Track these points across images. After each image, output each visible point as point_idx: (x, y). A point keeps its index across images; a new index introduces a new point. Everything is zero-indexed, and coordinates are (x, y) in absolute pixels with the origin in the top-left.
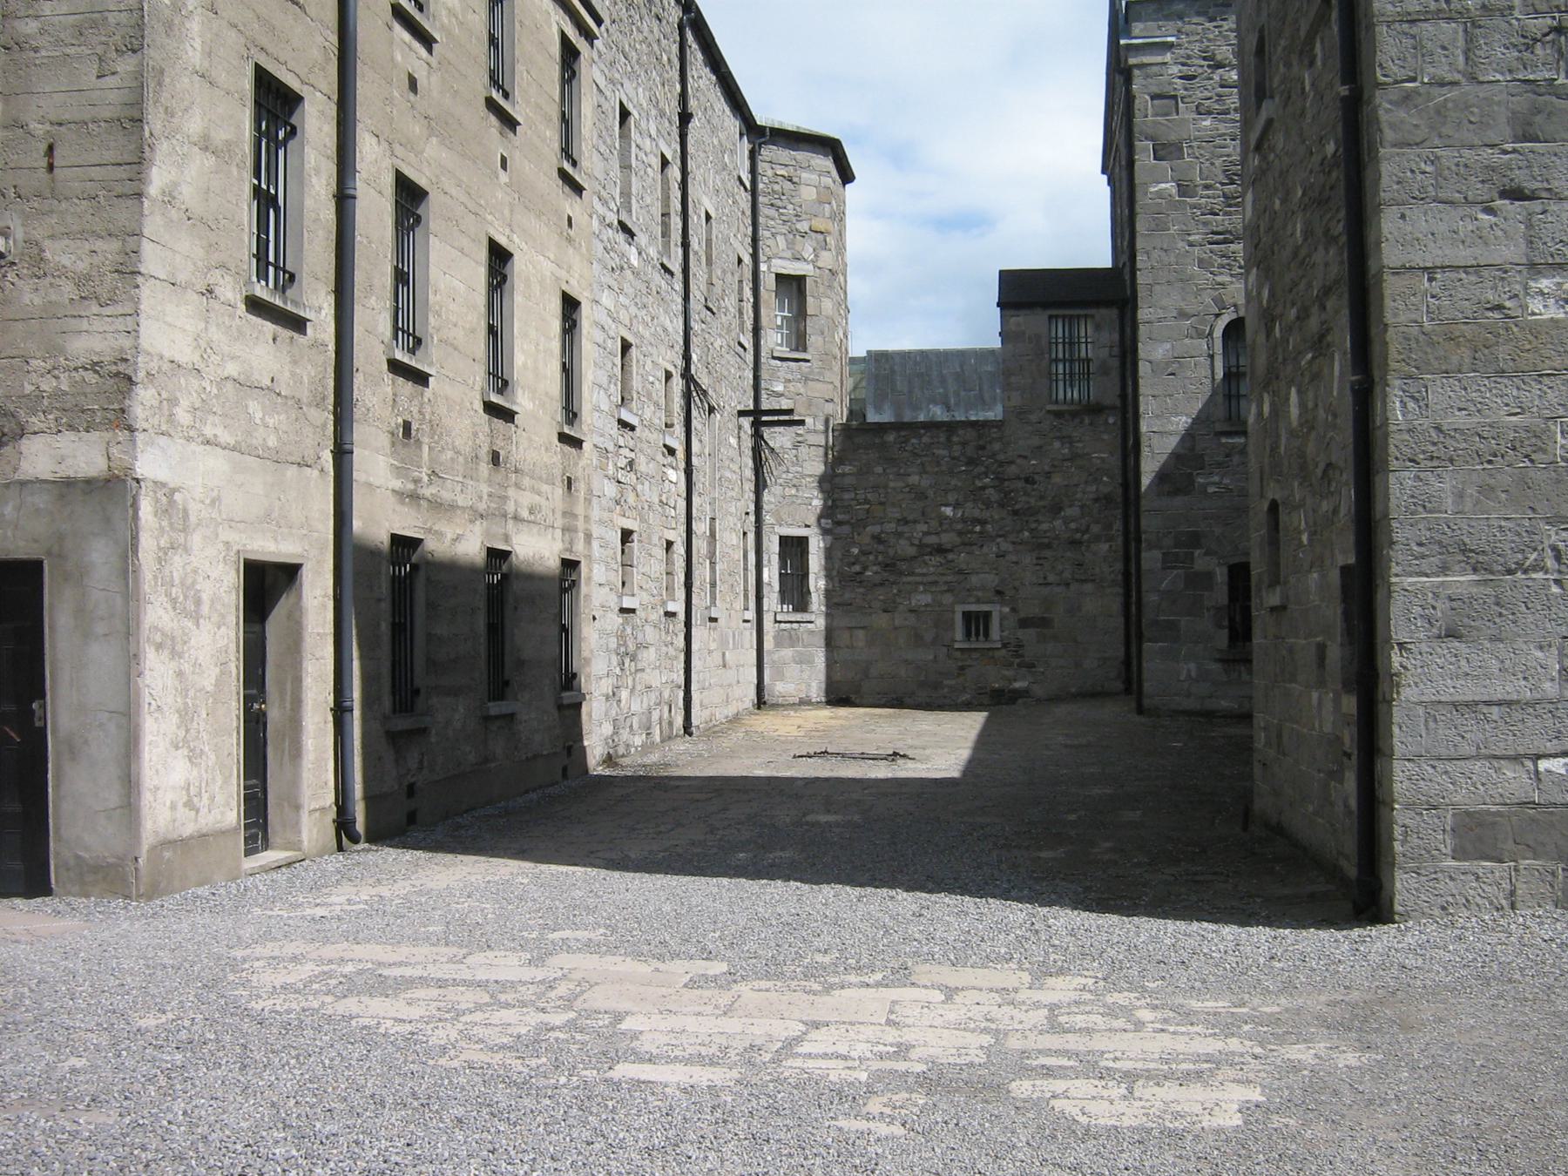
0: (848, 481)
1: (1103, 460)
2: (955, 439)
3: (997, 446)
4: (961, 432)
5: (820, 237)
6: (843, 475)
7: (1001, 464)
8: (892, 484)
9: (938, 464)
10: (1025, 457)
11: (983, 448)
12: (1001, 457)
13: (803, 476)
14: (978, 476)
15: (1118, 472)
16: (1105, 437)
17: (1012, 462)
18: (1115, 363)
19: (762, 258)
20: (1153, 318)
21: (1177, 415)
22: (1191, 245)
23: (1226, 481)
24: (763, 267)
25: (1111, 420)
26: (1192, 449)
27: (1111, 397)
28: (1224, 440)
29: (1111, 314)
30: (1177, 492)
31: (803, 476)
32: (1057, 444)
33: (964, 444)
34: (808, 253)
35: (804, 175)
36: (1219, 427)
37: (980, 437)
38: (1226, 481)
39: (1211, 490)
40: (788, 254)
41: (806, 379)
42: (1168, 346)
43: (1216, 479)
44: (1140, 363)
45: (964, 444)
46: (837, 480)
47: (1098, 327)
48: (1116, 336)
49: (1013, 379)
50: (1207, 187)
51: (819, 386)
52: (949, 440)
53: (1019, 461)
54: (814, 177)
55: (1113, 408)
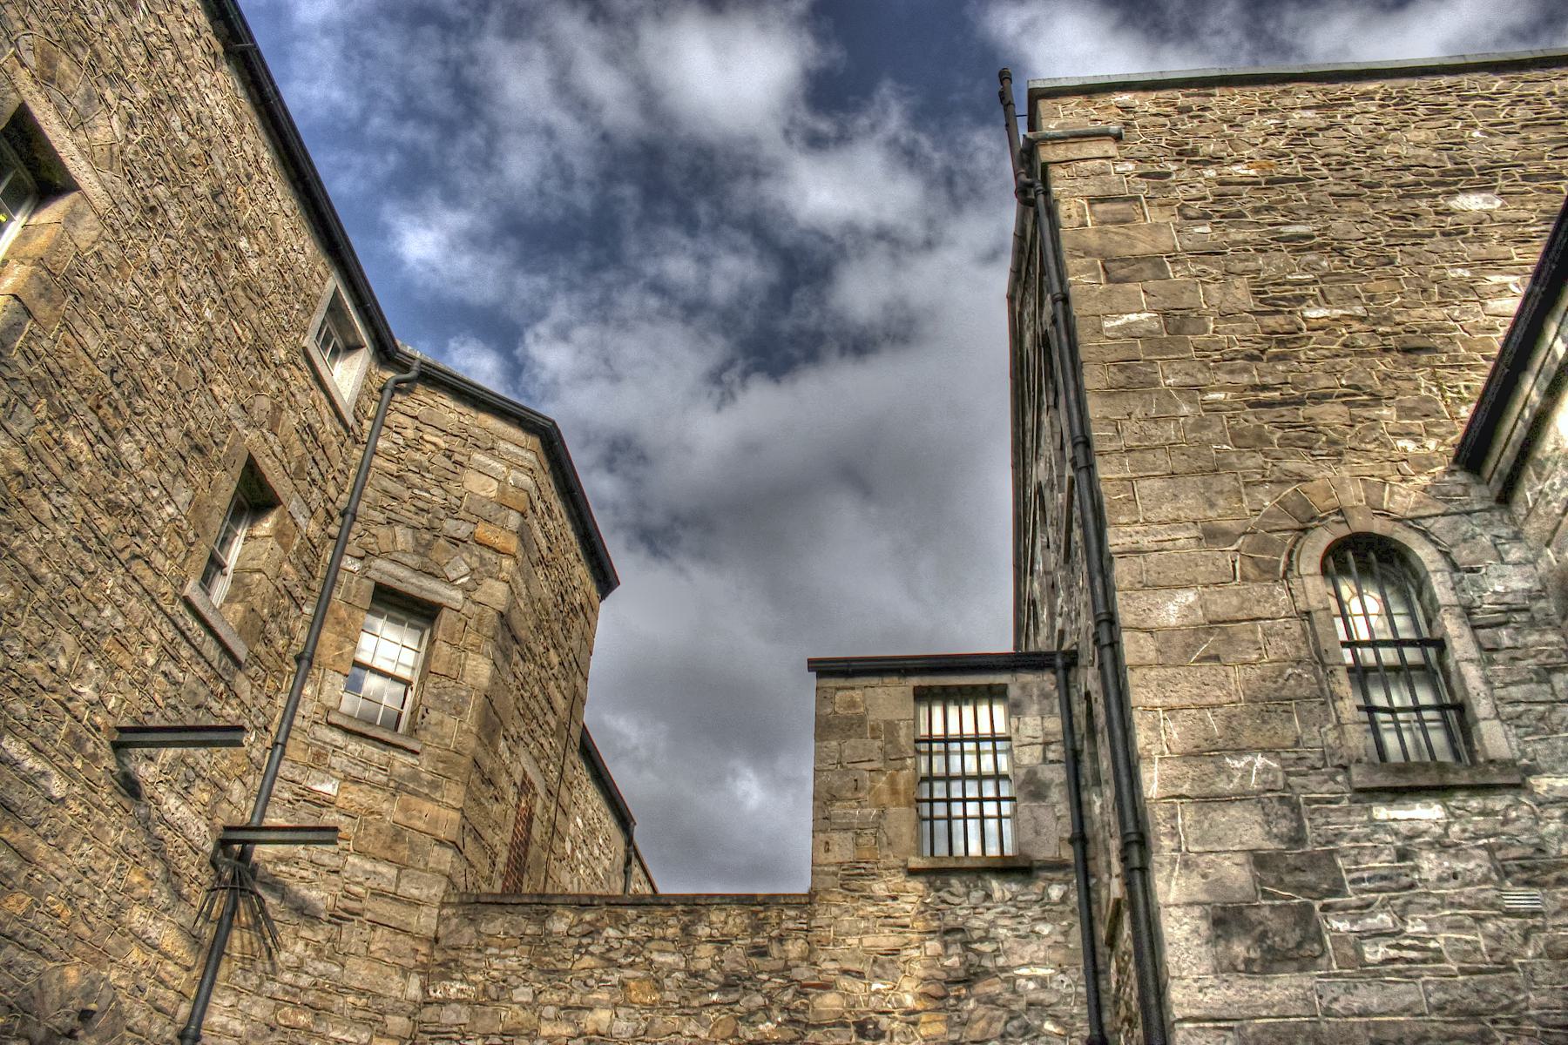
0: (449, 1016)
1: (1043, 983)
2: (703, 931)
3: (795, 948)
4: (716, 917)
5: (488, 554)
6: (442, 1003)
7: (802, 990)
8: (546, 1029)
9: (659, 987)
10: (860, 975)
11: (761, 952)
12: (803, 973)
13: (342, 990)
14: (748, 1018)
15: (1078, 1009)
16: (1045, 929)
17: (826, 987)
18: (1056, 775)
19: (352, 548)
20: (1145, 542)
21: (1239, 752)
22: (1214, 408)
23: (1416, 927)
24: (350, 564)
25: (1055, 892)
26: (1297, 839)
27: (1052, 842)
28: (1381, 812)
29: (1047, 680)
30: (1272, 960)
31: (342, 990)
32: (933, 946)
33: (721, 943)
34: (459, 568)
35: (478, 457)
36: (1359, 777)
37: (757, 928)
38: (1416, 927)
39: (1374, 953)
40: (413, 561)
41: (397, 788)
42: (1190, 597)
43: (1384, 920)
44: (1125, 637)
45: (721, 943)
46: (428, 1013)
47: (1015, 709)
48: (1055, 724)
49: (837, 809)
50: (1224, 316)
51: (428, 807)
52: (685, 929)
53: (844, 982)
54: (500, 467)
55: (1058, 866)
